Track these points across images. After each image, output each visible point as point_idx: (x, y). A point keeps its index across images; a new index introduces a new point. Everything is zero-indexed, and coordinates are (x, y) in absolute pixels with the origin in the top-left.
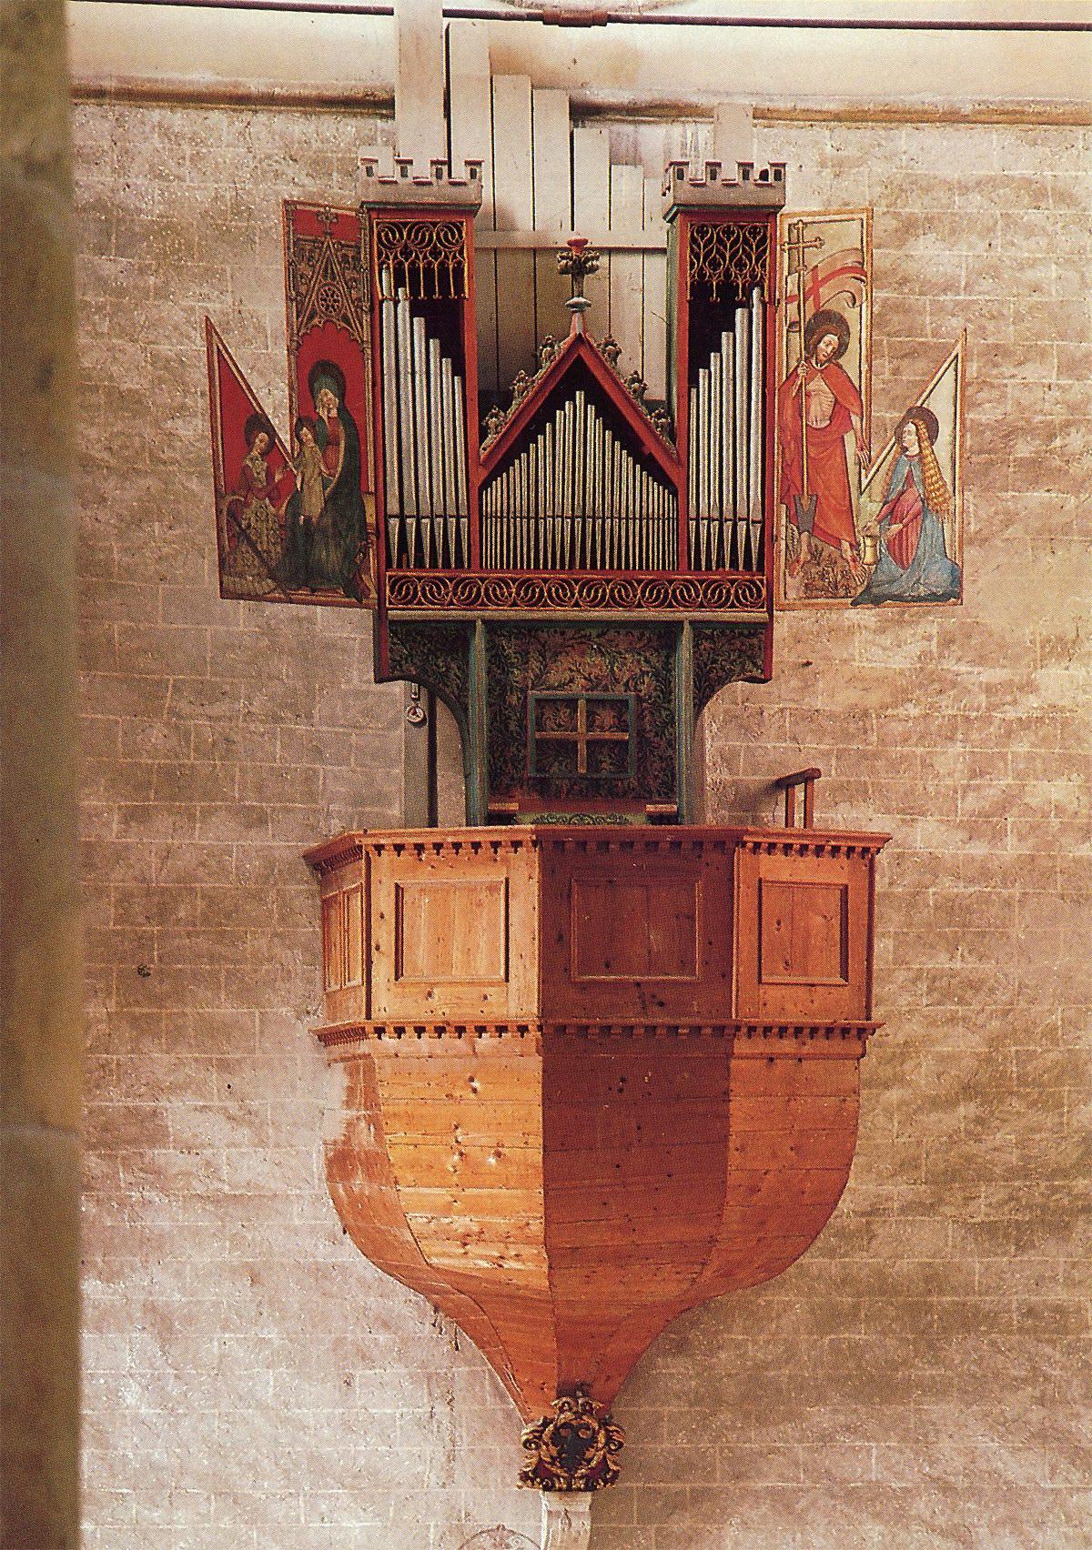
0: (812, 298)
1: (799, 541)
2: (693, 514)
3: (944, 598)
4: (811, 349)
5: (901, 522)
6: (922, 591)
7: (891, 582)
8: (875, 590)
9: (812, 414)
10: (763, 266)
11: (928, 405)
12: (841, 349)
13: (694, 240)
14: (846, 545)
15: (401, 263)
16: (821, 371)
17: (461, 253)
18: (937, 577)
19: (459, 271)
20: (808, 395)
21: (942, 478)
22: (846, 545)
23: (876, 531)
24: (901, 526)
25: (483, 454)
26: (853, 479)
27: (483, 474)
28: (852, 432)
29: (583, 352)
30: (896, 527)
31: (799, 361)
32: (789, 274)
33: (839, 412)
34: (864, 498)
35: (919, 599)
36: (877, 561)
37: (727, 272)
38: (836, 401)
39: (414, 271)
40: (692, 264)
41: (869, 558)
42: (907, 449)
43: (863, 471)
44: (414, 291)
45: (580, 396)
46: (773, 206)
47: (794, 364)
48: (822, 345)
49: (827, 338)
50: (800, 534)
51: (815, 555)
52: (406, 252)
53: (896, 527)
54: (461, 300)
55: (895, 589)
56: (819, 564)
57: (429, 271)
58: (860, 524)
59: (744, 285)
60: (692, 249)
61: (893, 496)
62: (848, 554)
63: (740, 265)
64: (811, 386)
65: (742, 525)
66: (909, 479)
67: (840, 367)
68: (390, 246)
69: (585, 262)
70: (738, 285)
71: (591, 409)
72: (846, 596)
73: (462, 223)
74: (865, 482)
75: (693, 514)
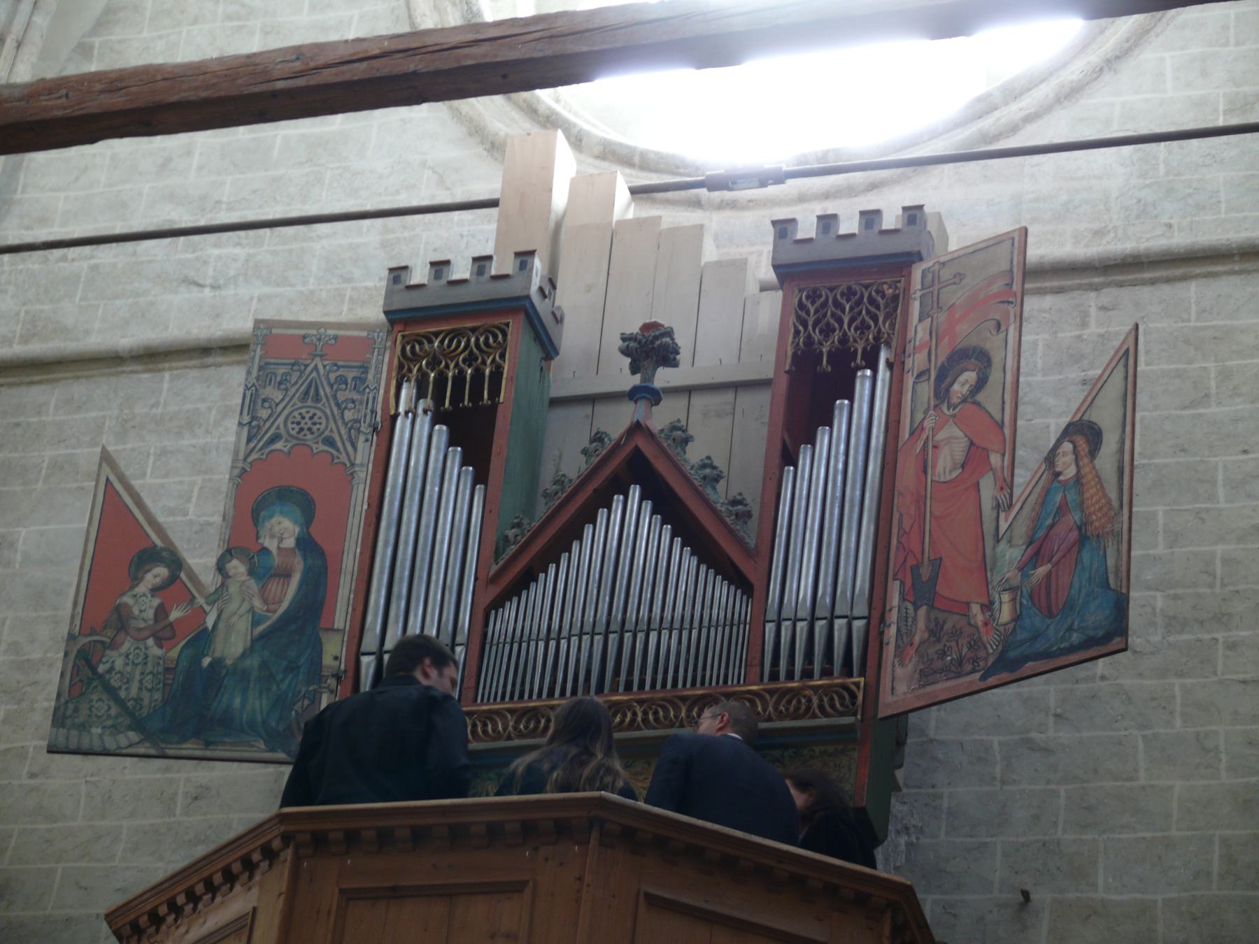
0: (947, 338)
1: (915, 619)
2: (772, 614)
3: (1107, 638)
4: (942, 394)
5: (1049, 561)
6: (1075, 638)
7: (1034, 638)
8: (1012, 654)
9: (940, 467)
10: (892, 326)
11: (1095, 416)
12: (981, 383)
13: (801, 306)
14: (975, 609)
15: (425, 376)
16: (954, 416)
17: (502, 356)
18: (1096, 616)
19: (497, 375)
20: (935, 447)
21: (1105, 495)
22: (975, 609)
23: (1016, 581)
24: (1049, 566)
25: (494, 568)
26: (988, 526)
27: (494, 592)
28: (991, 473)
29: (640, 442)
30: (1042, 570)
31: (926, 412)
32: (920, 320)
33: (975, 458)
34: (1002, 546)
35: (1073, 649)
36: (1017, 618)
37: (844, 340)
38: (972, 444)
39: (441, 381)
40: (797, 333)
41: (1005, 614)
42: (1059, 474)
43: (1002, 515)
44: (439, 398)
45: (635, 492)
46: (909, 254)
47: (919, 416)
48: (956, 387)
49: (962, 378)
50: (916, 610)
51: (935, 631)
52: (434, 363)
53: (1042, 570)
54: (494, 407)
55: (1040, 646)
56: (939, 641)
57: (459, 379)
58: (995, 579)
59: (864, 350)
60: (798, 317)
61: (1041, 534)
62: (980, 619)
63: (864, 327)
64: (940, 436)
65: (839, 624)
66: (1062, 510)
67: (978, 404)
68: (416, 358)
69: (652, 342)
70: (856, 351)
71: (647, 506)
72: (973, 671)
73: (507, 325)
74: (1003, 526)
75: (772, 614)
